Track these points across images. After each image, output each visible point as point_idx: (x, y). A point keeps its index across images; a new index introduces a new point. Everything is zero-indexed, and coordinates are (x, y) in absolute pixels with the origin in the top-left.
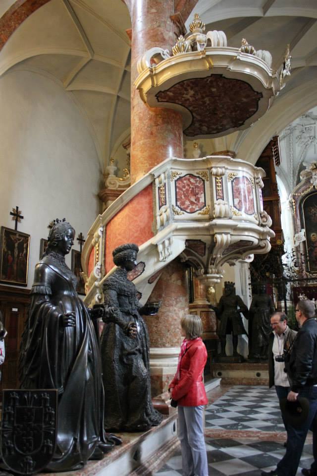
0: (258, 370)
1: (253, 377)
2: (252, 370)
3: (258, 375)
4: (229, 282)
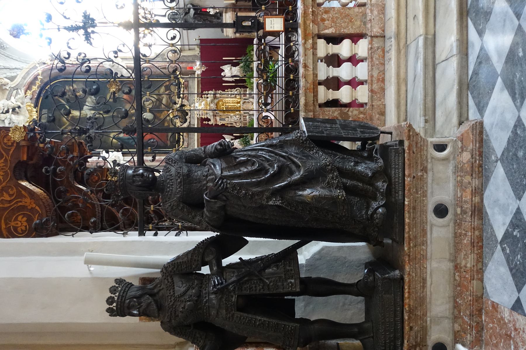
0: (424, 212)
1: (451, 228)
2: (424, 232)
3: (441, 211)
4: (110, 301)
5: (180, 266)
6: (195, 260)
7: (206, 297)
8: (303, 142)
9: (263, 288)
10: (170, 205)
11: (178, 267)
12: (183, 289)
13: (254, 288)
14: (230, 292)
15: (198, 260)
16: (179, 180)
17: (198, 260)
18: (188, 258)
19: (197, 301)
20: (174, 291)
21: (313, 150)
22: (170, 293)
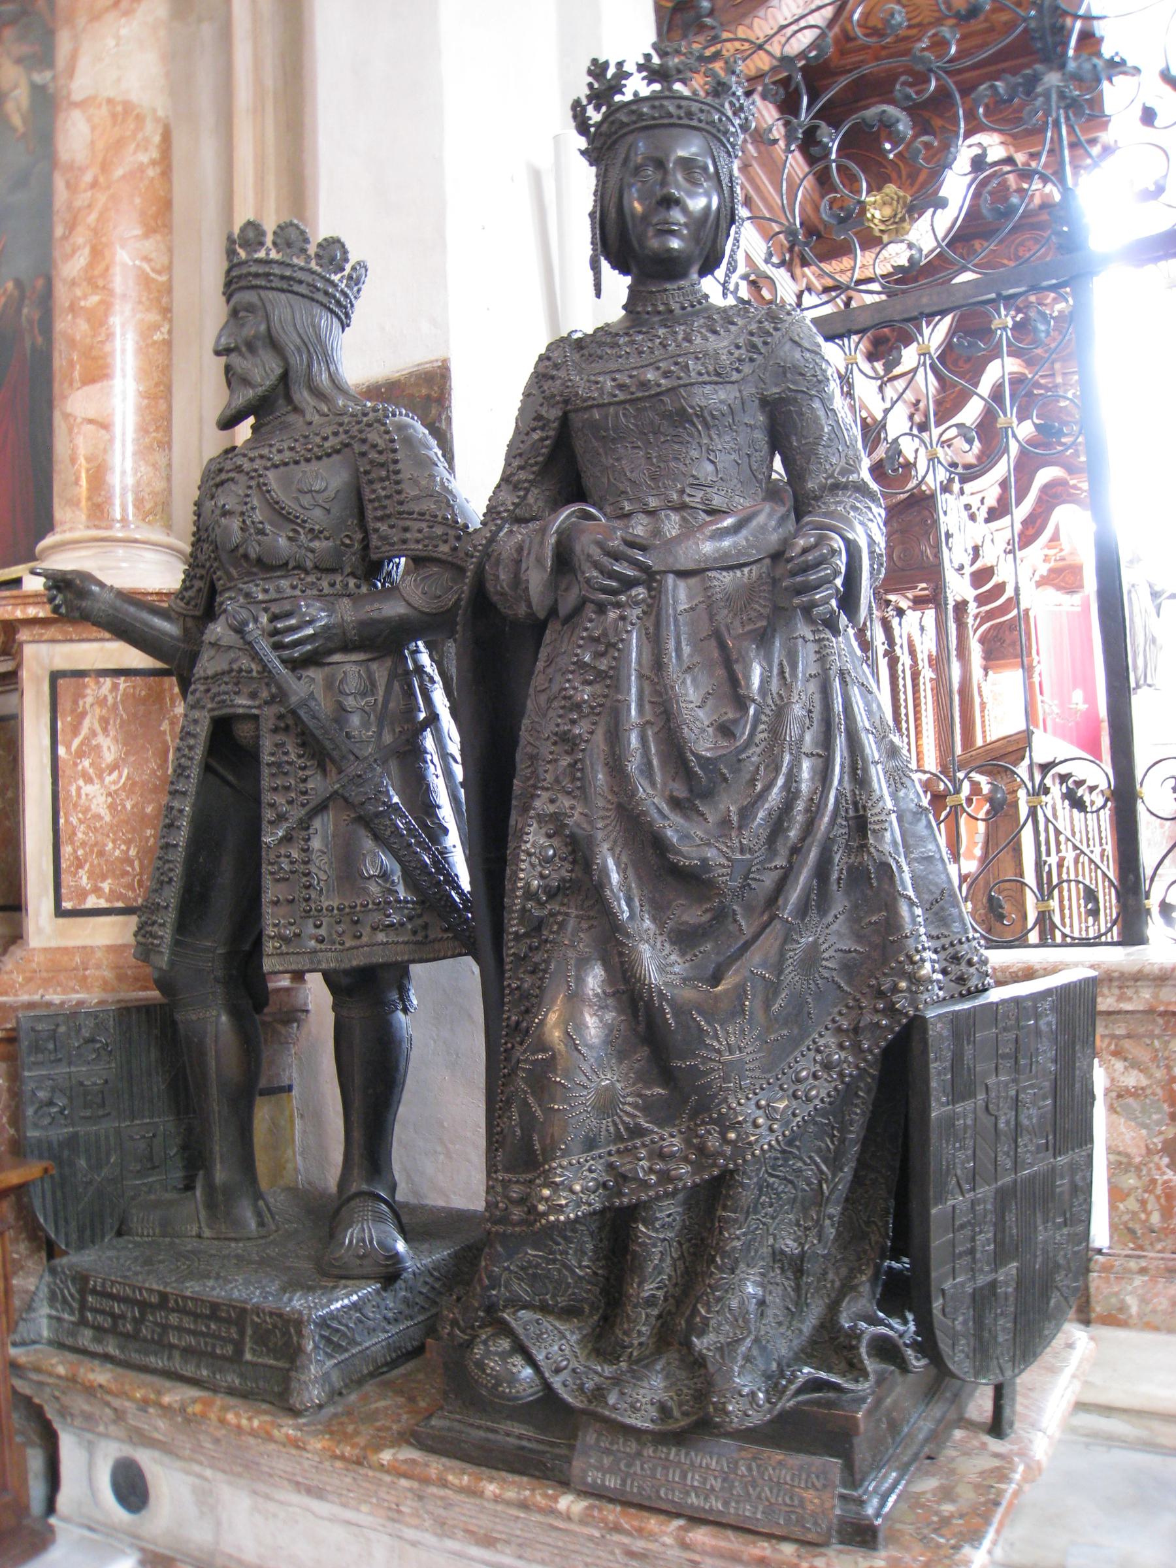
5: (384, 473)
6: (406, 529)
7: (266, 591)
8: (881, 994)
11: (382, 465)
16: (650, 376)
18: (417, 498)
20: (286, 464)
21: (841, 1046)
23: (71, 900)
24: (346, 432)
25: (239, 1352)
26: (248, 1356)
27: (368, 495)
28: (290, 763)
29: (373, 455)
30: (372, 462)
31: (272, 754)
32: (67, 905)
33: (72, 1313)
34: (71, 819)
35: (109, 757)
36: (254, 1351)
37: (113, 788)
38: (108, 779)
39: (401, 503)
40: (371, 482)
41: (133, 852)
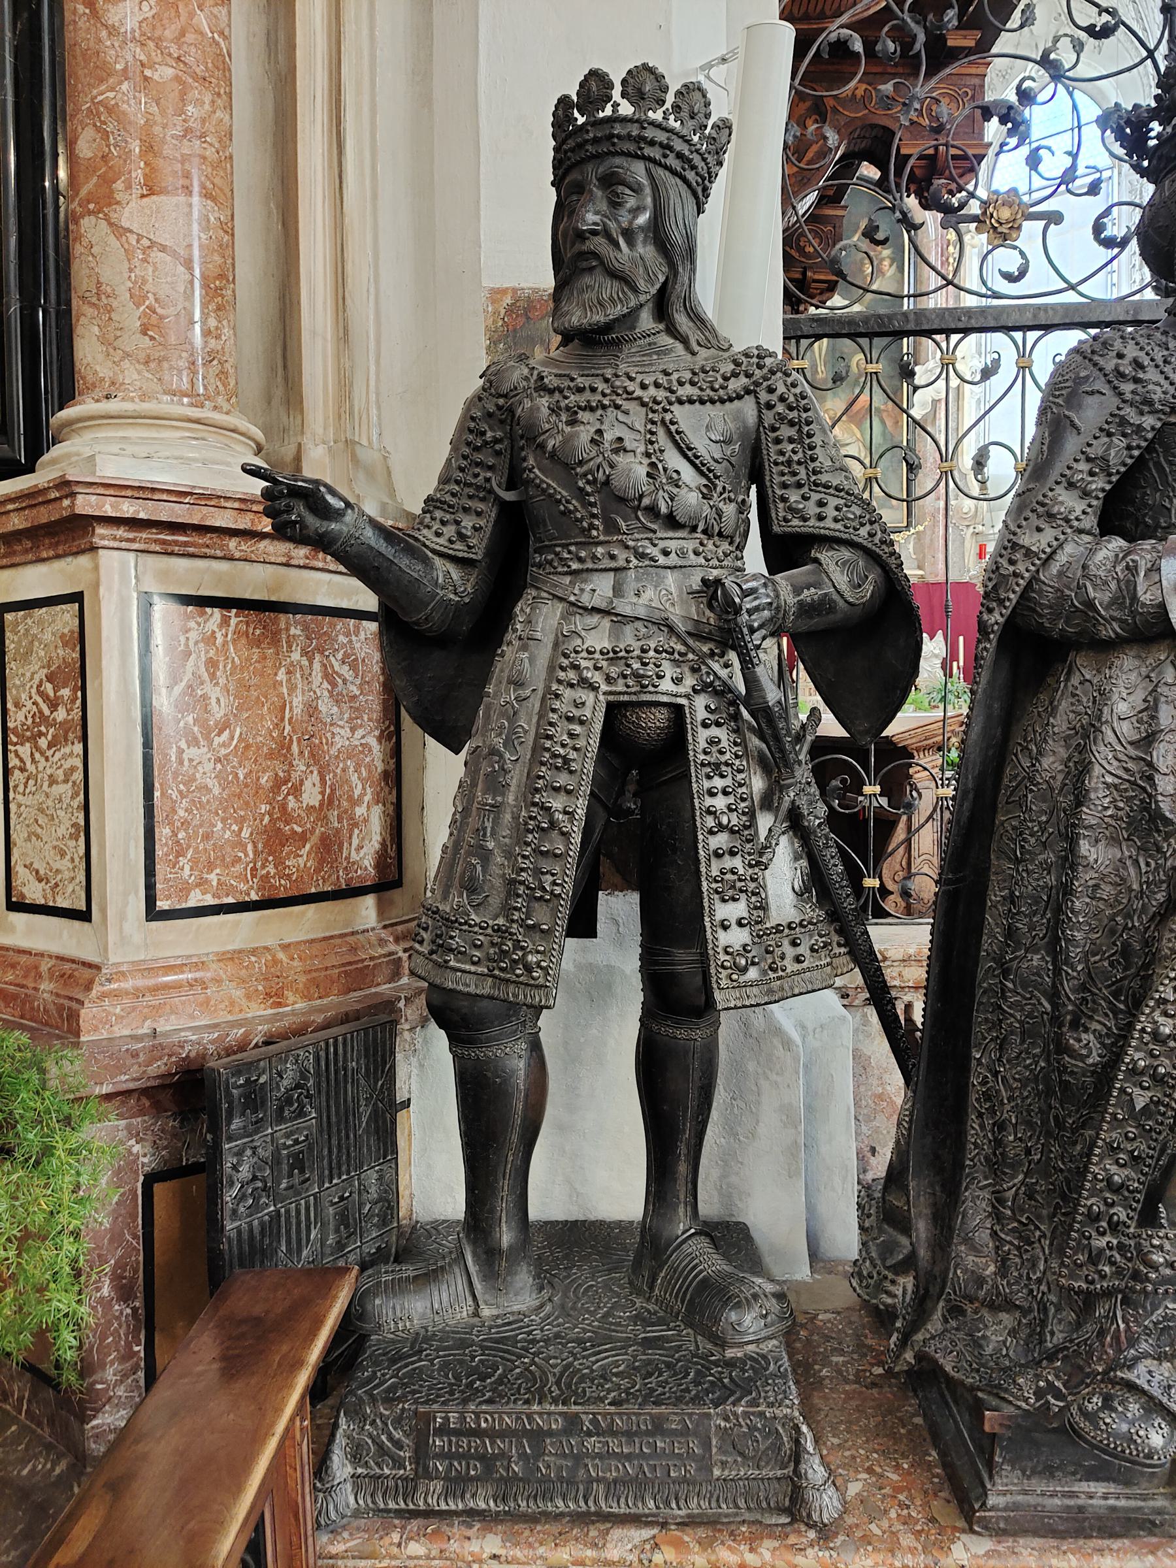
9: (721, 827)
10: (1138, 365)
12: (703, 446)
13: (718, 783)
14: (694, 670)
15: (821, 518)
17: (821, 518)
19: (652, 510)
20: (691, 402)
22: (681, 384)
23: (168, 897)
24: (748, 376)
25: (705, 1466)
26: (717, 1472)
27: (771, 452)
28: (727, 764)
29: (780, 408)
30: (781, 418)
31: (705, 753)
32: (162, 904)
33: (399, 1463)
34: (166, 791)
35: (218, 713)
36: (724, 1464)
37: (223, 752)
38: (217, 740)
39: (815, 472)
40: (778, 441)
41: (245, 833)
